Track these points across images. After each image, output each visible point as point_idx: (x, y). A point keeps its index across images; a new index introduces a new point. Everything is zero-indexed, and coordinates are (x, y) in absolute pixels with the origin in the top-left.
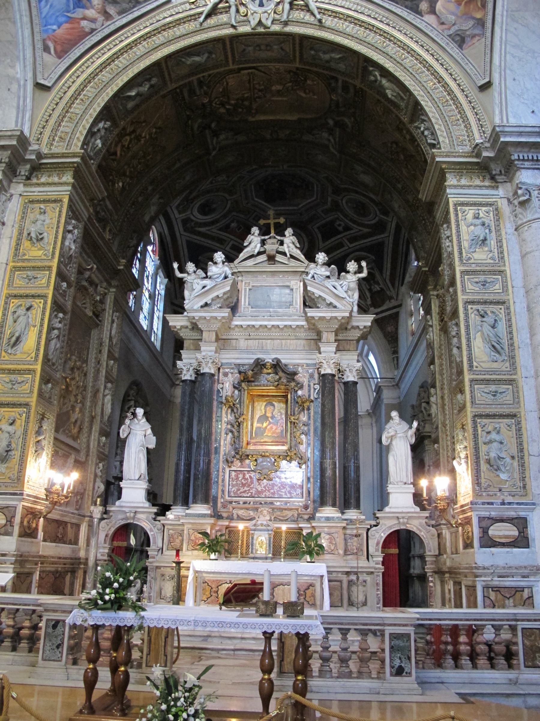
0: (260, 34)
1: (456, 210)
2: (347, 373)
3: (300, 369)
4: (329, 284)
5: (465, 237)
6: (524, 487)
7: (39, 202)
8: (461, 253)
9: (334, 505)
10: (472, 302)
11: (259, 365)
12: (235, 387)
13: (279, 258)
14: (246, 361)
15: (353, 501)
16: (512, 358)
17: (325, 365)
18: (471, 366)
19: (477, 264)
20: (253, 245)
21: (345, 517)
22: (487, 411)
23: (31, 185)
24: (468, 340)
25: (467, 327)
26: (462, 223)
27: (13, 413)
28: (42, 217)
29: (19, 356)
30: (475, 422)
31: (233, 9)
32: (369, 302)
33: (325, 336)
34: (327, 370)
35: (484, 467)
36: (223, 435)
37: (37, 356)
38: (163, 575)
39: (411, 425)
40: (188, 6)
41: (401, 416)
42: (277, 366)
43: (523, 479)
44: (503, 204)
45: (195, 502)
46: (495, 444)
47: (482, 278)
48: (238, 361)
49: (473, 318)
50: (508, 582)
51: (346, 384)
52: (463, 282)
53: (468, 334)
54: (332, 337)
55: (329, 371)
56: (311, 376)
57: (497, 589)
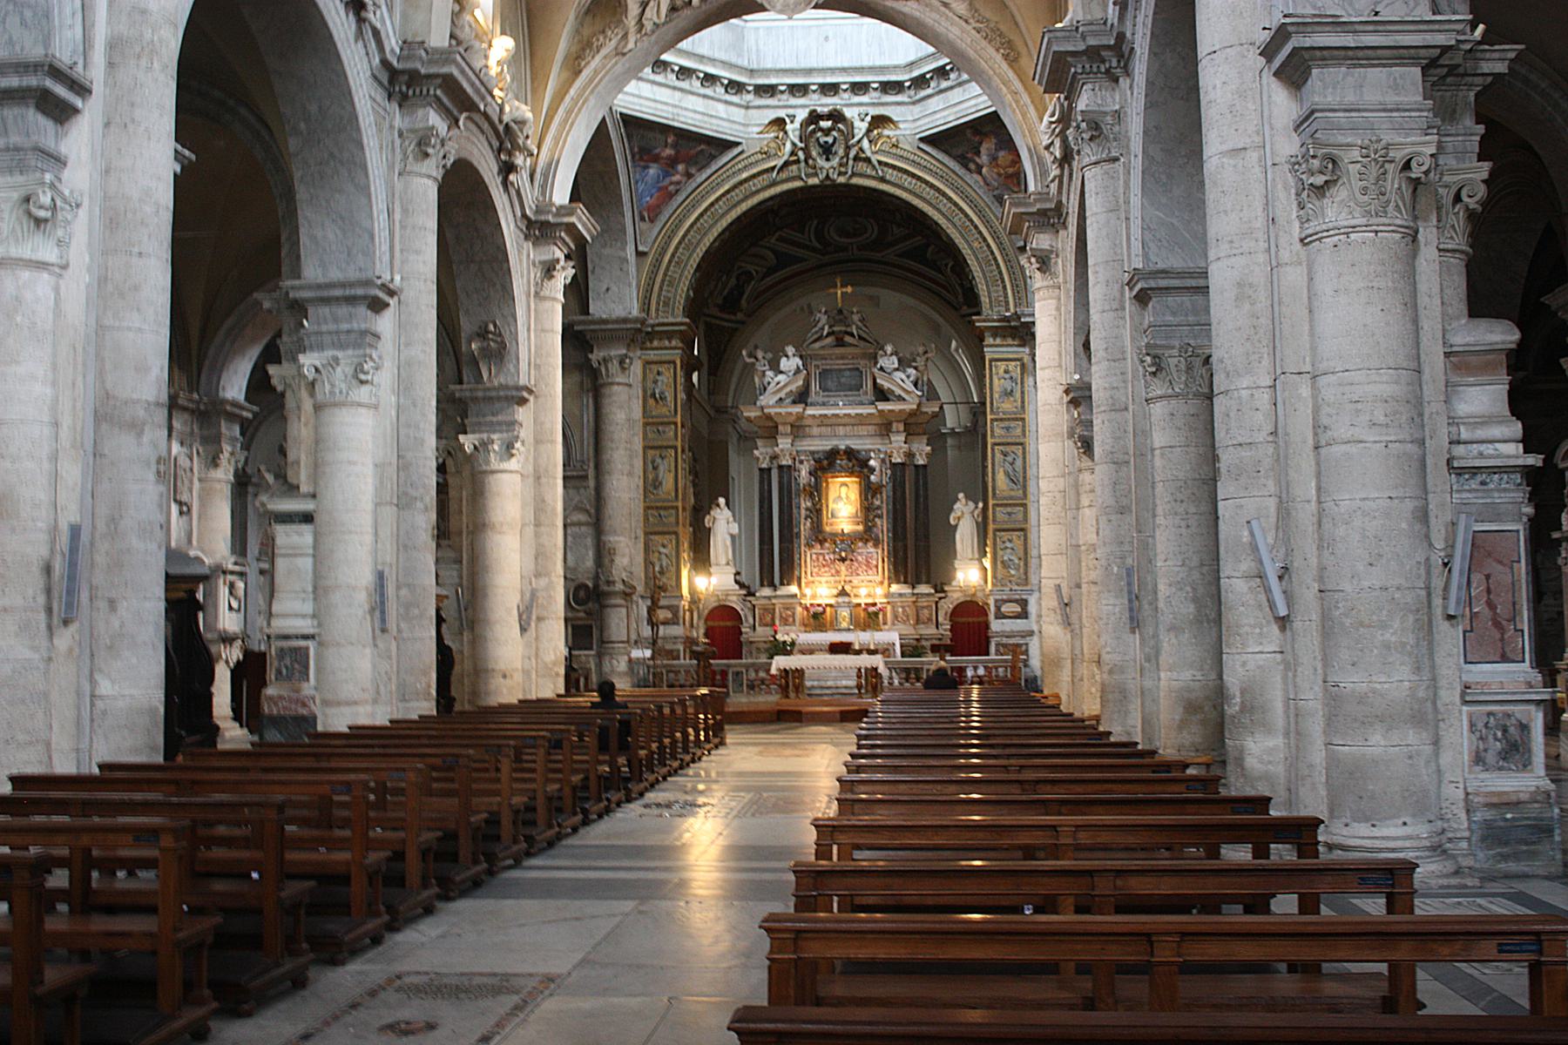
0: (827, 186)
1: (991, 366)
2: (918, 456)
3: (872, 455)
4: (899, 375)
5: (996, 388)
6: (1026, 579)
7: (656, 363)
8: (992, 404)
9: (905, 582)
10: (999, 444)
11: (833, 454)
12: (810, 474)
13: (848, 339)
14: (821, 448)
15: (924, 579)
16: (1025, 487)
17: (895, 454)
18: (994, 494)
19: (1004, 413)
20: (820, 325)
21: (916, 591)
22: (1005, 527)
23: (647, 349)
24: (993, 473)
25: (993, 465)
26: (995, 377)
27: (665, 539)
28: (659, 378)
29: (663, 496)
30: (995, 535)
31: (803, 164)
32: (961, 299)
33: (894, 425)
34: (898, 459)
35: (999, 565)
36: (803, 520)
37: (677, 496)
38: (758, 649)
39: (976, 504)
40: (760, 156)
41: (967, 497)
42: (850, 453)
43: (1026, 573)
44: (1027, 359)
45: (782, 584)
46: (1009, 551)
47: (1006, 424)
48: (812, 448)
49: (998, 455)
50: (1012, 641)
51: (917, 467)
52: (992, 428)
53: (993, 469)
54: (901, 427)
55: (899, 460)
56: (883, 461)
57: (1005, 646)
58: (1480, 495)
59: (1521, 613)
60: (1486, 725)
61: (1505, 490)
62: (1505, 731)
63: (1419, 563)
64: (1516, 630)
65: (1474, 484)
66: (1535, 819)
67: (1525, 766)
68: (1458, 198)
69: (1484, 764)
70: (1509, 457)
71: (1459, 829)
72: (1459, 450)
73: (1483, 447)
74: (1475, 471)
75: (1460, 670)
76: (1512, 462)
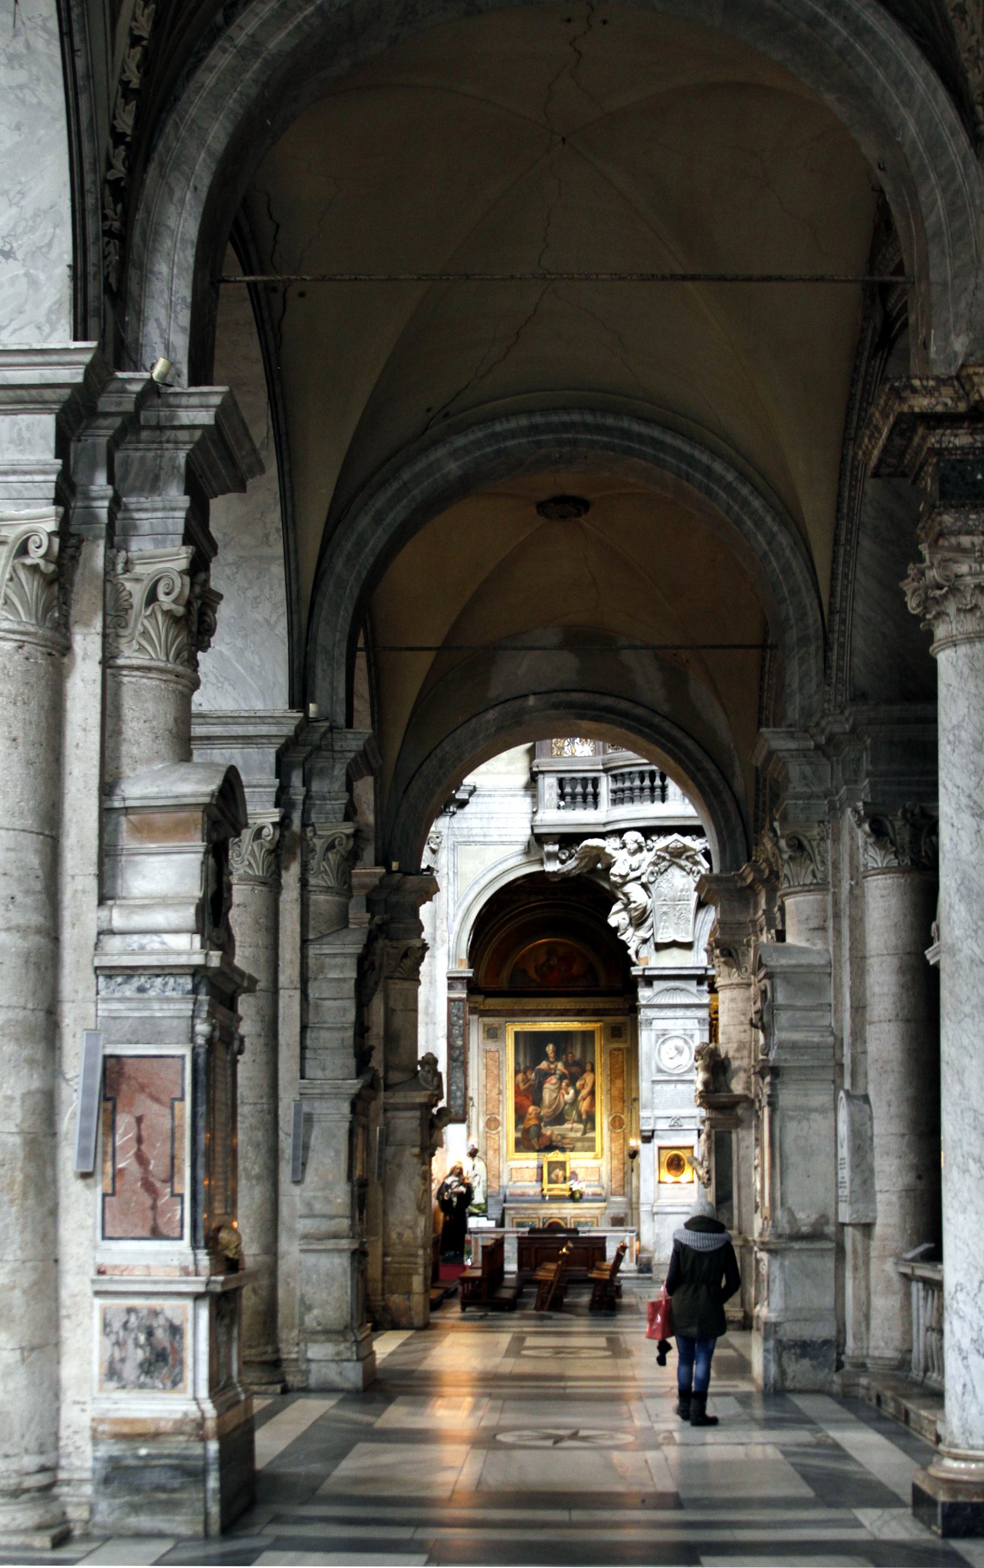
58: (133, 1005)
59: (181, 1171)
60: (125, 1326)
61: (169, 1000)
62: (150, 1333)
63: (11, 1099)
64: (173, 1195)
65: (129, 990)
66: (177, 1457)
67: (175, 1384)
68: (152, 598)
69: (120, 1378)
70: (179, 953)
71: (81, 1468)
72: (114, 943)
73: (145, 939)
74: (130, 972)
75: (95, 1247)
76: (183, 960)
